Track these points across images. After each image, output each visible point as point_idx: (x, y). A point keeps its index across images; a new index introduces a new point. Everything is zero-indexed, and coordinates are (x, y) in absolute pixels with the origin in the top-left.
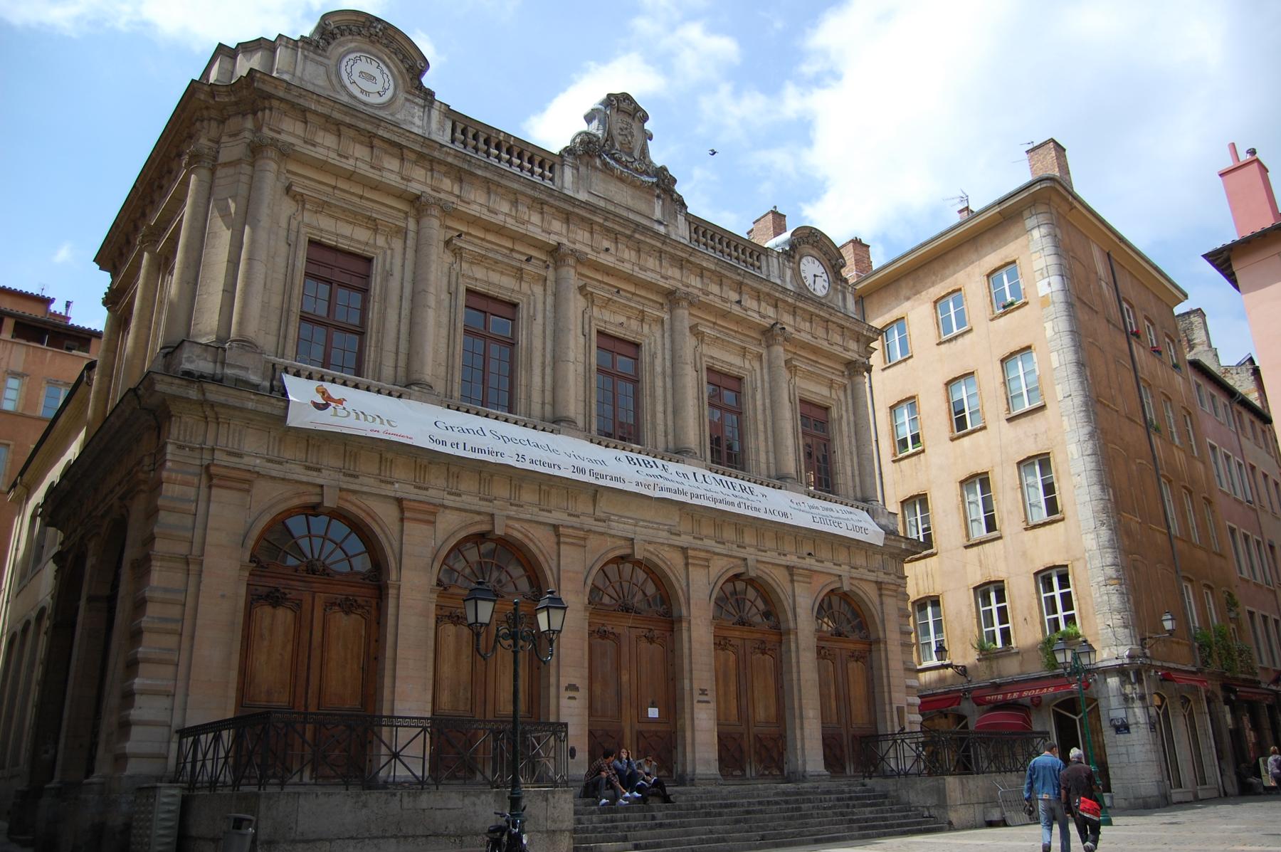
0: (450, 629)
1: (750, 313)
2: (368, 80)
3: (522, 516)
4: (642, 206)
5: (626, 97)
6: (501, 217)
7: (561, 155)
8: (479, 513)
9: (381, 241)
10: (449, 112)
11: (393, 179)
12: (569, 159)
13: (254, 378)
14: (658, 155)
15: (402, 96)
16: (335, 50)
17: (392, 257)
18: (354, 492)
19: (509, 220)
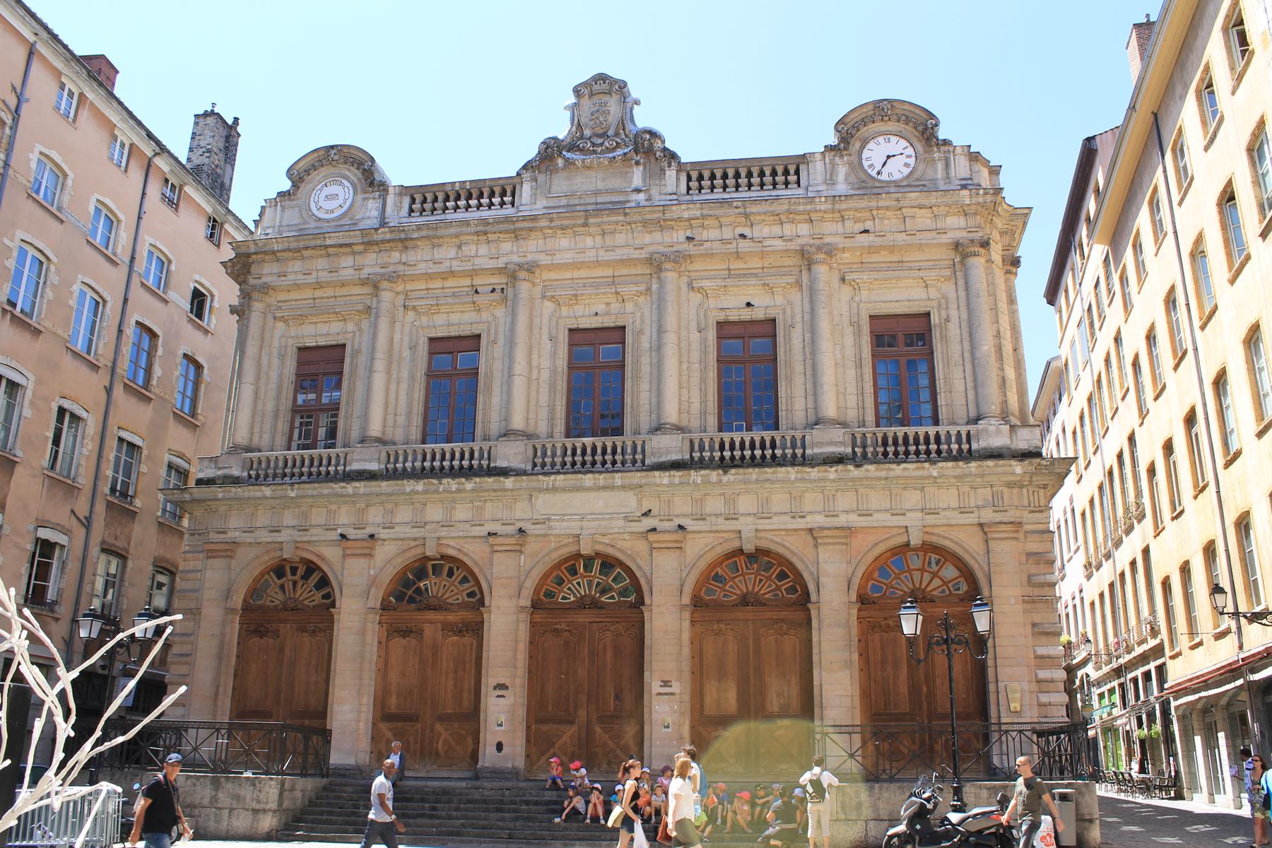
0: (398, 643)
1: (767, 243)
2: (333, 198)
3: (453, 535)
4: (616, 183)
5: (601, 78)
6: (447, 264)
7: (518, 174)
8: (415, 539)
9: (351, 327)
10: (404, 190)
11: (348, 274)
12: (526, 176)
13: (236, 472)
14: (643, 119)
15: (360, 197)
16: (304, 188)
17: (360, 336)
18: (309, 542)
19: (454, 263)
